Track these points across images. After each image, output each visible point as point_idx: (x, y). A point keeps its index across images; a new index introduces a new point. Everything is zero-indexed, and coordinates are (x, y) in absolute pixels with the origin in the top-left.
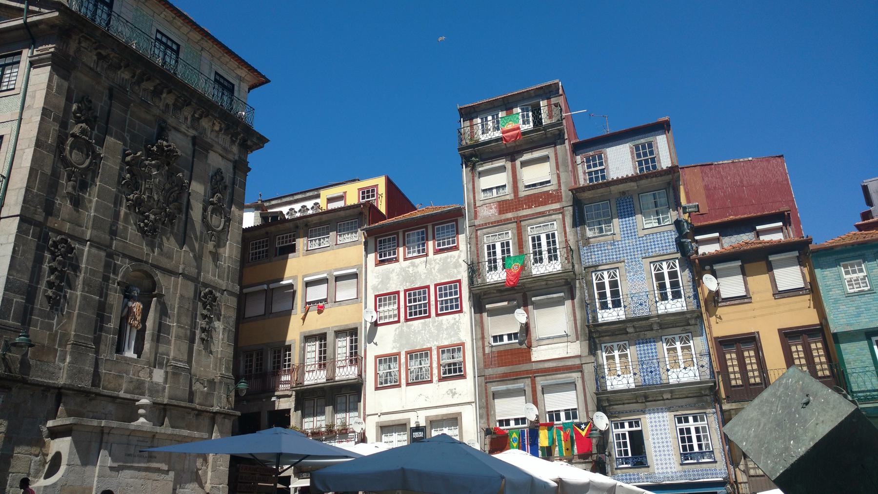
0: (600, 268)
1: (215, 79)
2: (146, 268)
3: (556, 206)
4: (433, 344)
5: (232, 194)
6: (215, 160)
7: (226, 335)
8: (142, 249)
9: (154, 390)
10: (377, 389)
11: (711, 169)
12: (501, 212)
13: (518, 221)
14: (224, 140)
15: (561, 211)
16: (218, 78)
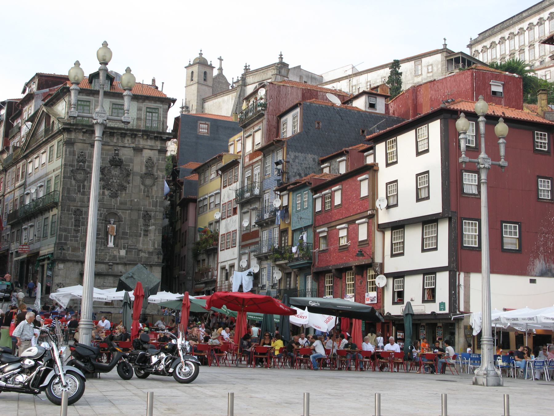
0: (266, 192)
1: (147, 112)
2: (112, 211)
3: (260, 157)
4: (231, 230)
5: (157, 166)
6: (147, 153)
7: (157, 232)
8: (112, 204)
9: (120, 258)
10: (221, 250)
11: (434, 84)
12: (250, 160)
13: (252, 165)
14: (150, 143)
15: (260, 160)
16: (148, 110)
